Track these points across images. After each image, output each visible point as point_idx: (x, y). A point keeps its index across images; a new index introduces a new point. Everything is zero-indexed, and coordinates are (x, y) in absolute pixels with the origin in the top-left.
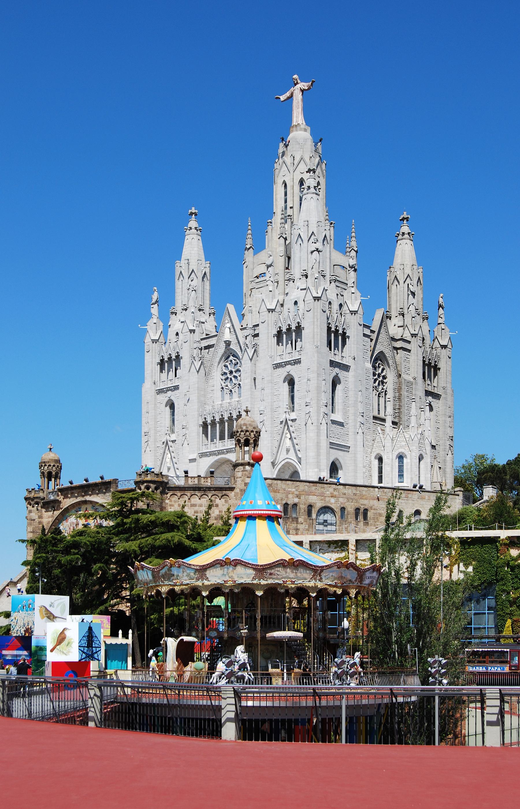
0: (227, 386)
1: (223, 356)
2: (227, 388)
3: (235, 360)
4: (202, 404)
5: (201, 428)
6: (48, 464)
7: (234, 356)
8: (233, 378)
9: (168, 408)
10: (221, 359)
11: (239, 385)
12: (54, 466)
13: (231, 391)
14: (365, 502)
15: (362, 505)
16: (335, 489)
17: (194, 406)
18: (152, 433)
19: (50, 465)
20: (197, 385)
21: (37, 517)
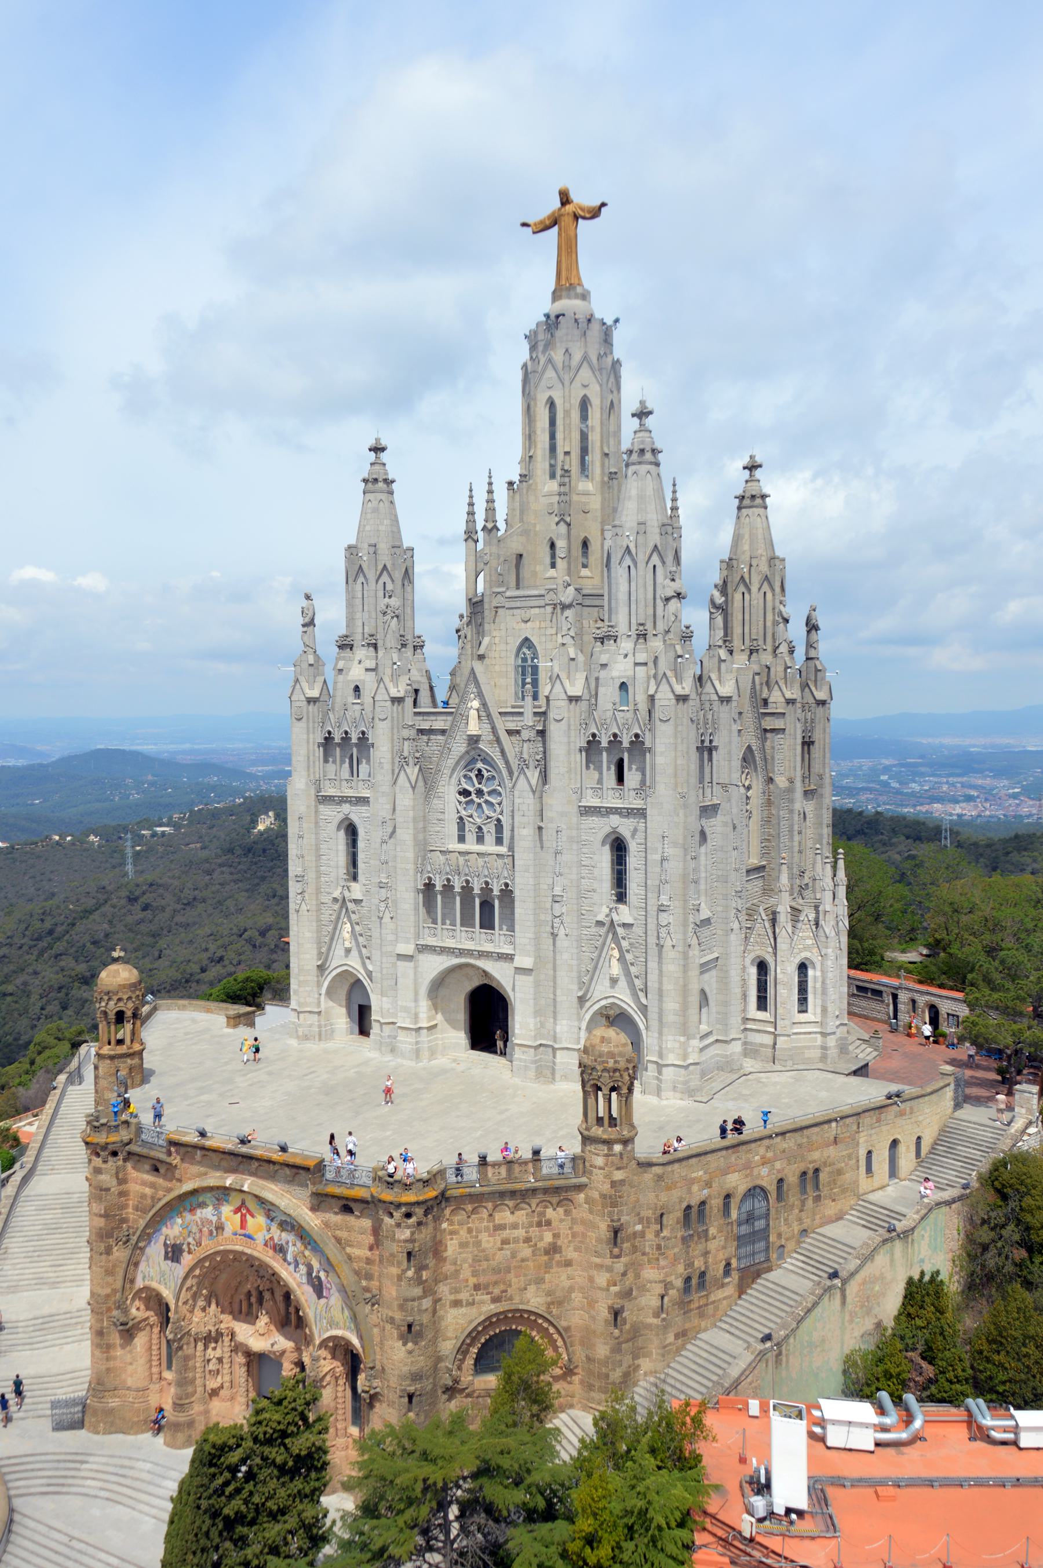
0: (471, 816)
1: (461, 758)
2: (471, 819)
3: (488, 771)
4: (424, 850)
5: (421, 895)
6: (115, 998)
7: (484, 761)
8: (484, 805)
9: (342, 834)
10: (457, 763)
11: (499, 820)
12: (130, 998)
13: (480, 828)
14: (816, 1155)
15: (811, 1162)
16: (768, 1147)
17: (405, 852)
18: (311, 876)
19: (120, 1000)
20: (411, 813)
21: (114, 1182)
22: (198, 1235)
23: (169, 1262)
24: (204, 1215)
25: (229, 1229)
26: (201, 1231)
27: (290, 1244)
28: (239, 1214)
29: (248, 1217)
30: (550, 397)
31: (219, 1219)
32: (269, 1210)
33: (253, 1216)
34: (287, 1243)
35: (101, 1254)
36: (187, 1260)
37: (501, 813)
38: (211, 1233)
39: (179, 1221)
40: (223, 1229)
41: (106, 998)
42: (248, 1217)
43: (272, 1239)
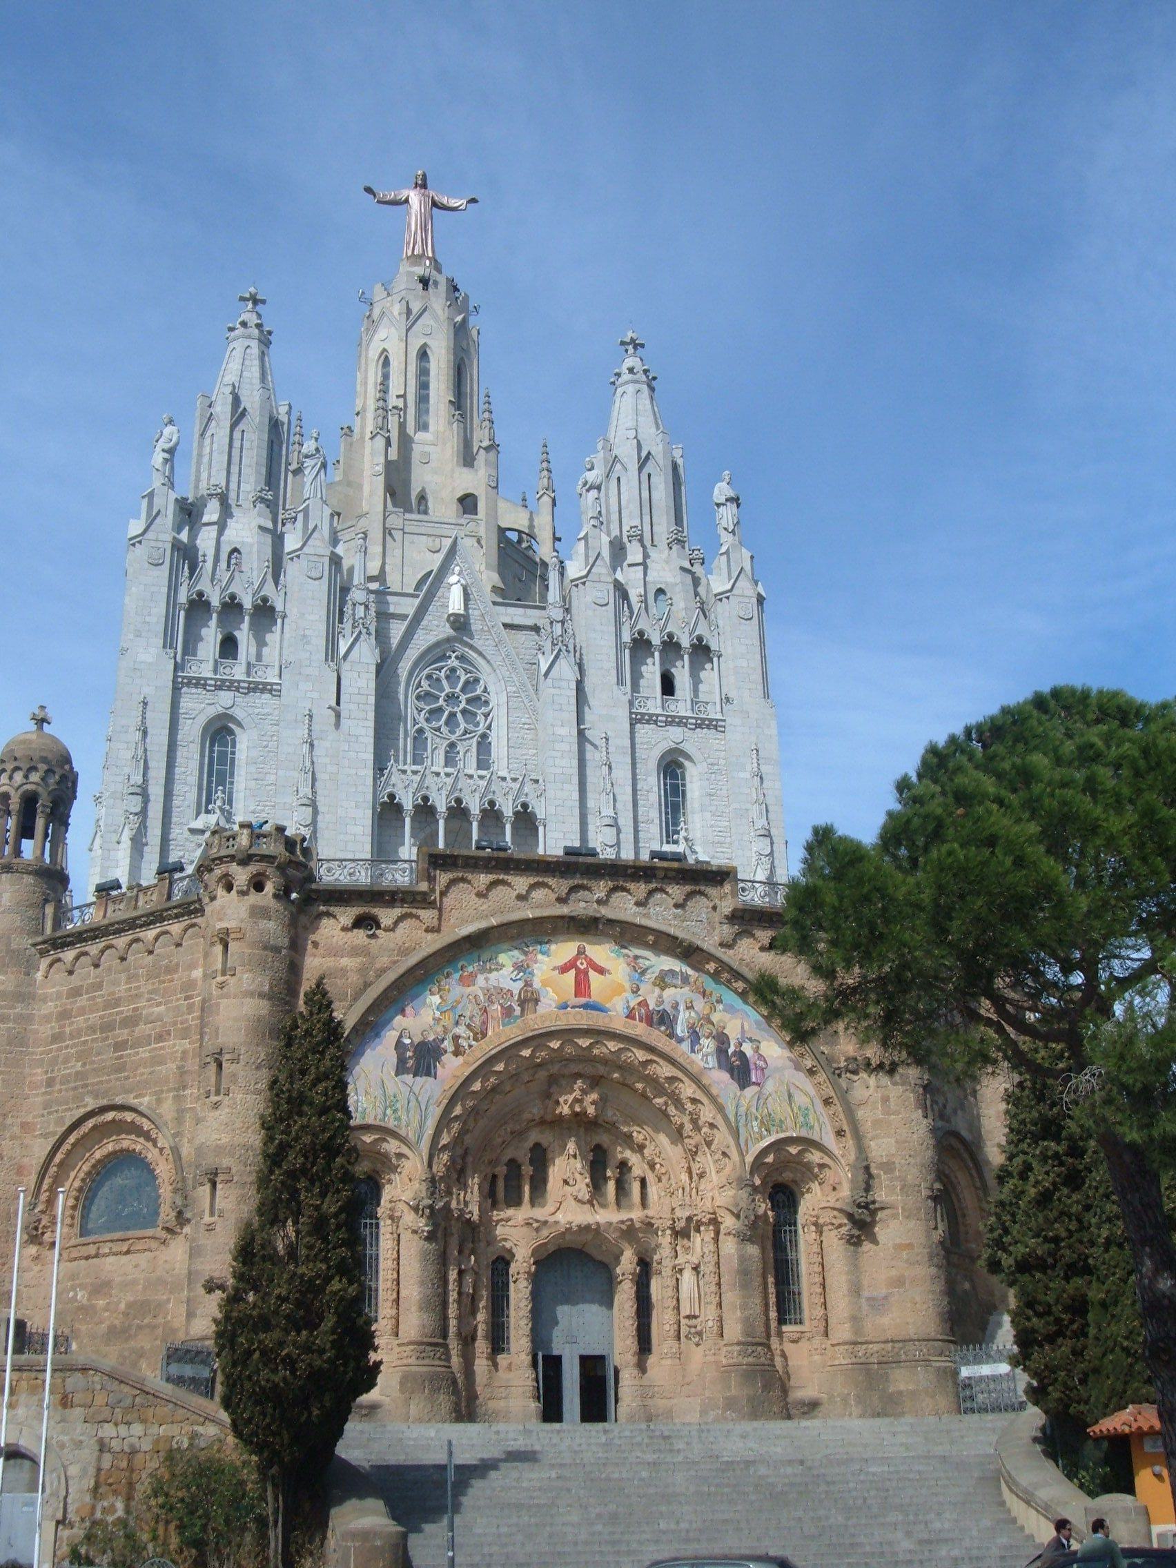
0: (438, 730)
8: (459, 716)
11: (484, 736)
20: (372, 699)
21: (286, 942)
22: (477, 1021)
23: (408, 1078)
24: (493, 982)
25: (549, 1001)
26: (485, 1011)
27: (682, 1008)
28: (572, 972)
29: (592, 973)
30: (425, 345)
31: (528, 984)
32: (636, 957)
33: (601, 971)
34: (676, 1006)
35: (258, 1068)
36: (452, 1069)
37: (489, 727)
38: (508, 1011)
39: (436, 999)
40: (537, 1001)
41: (43, 767)
42: (592, 973)
43: (643, 1004)
